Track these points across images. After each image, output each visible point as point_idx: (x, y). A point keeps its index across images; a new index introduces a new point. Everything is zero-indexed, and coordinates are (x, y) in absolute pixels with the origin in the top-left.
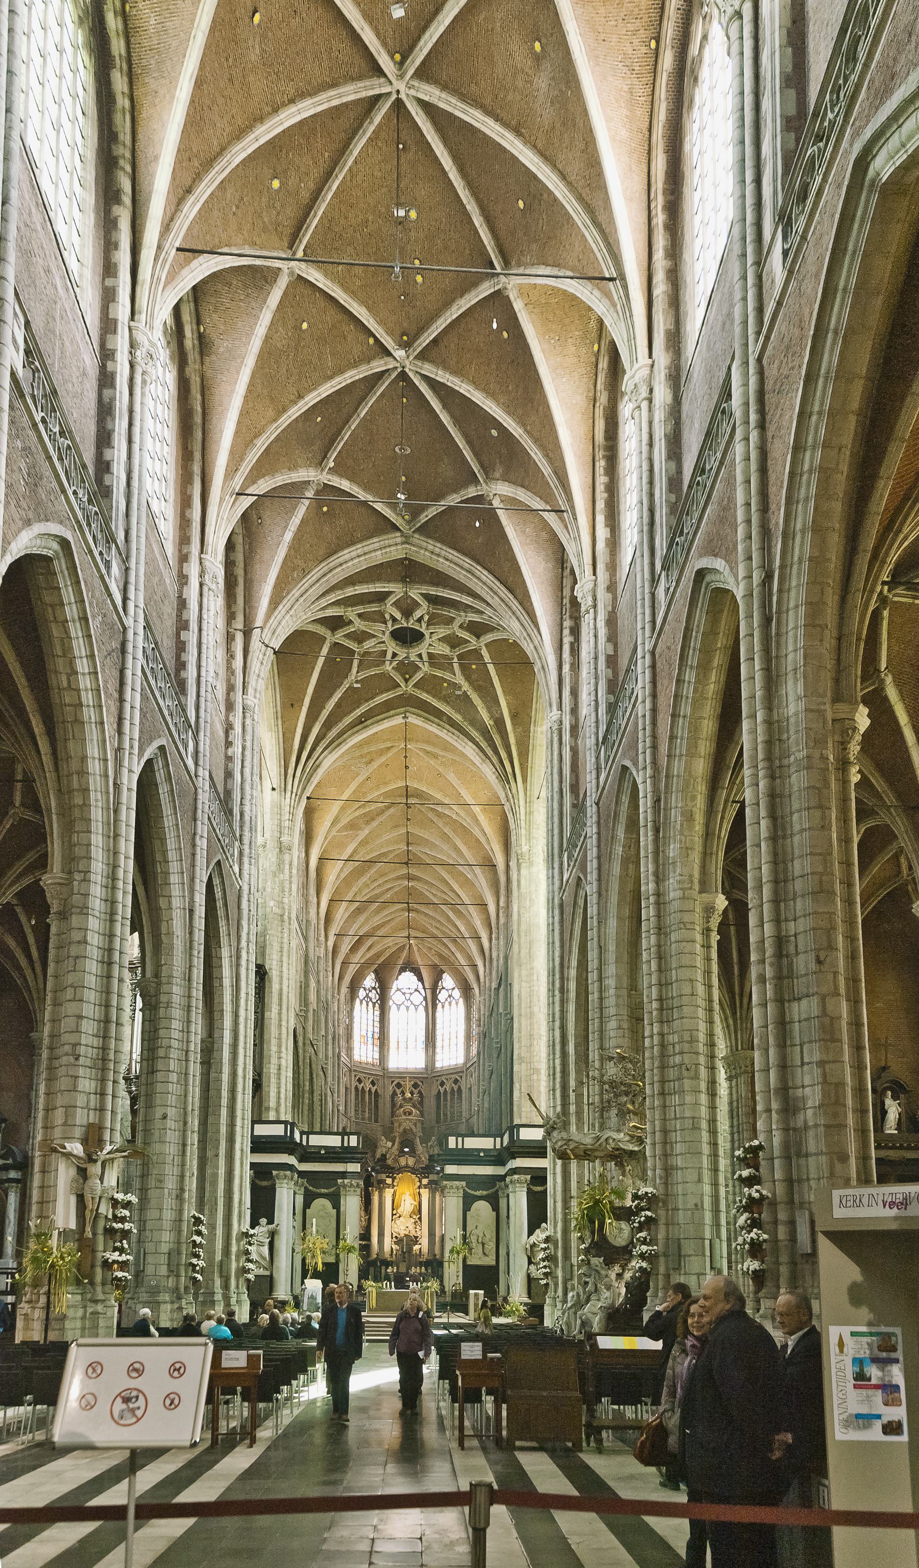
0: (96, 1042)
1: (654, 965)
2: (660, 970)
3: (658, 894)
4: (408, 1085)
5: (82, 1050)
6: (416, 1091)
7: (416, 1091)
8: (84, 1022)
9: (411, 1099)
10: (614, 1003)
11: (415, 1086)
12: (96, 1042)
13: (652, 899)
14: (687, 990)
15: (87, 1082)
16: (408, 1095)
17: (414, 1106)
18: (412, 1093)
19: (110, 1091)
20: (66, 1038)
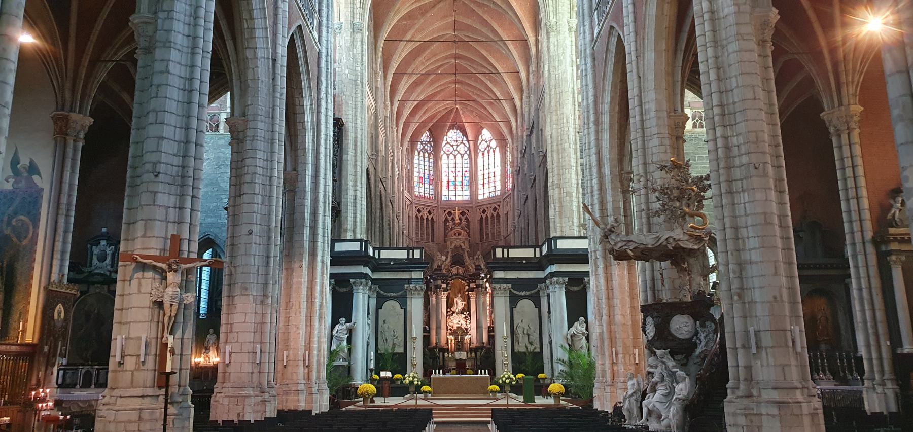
0: (177, 161)
1: (713, 75)
2: (719, 79)
3: (712, 12)
4: (457, 213)
5: (162, 168)
6: (463, 218)
7: (463, 218)
8: (165, 142)
9: (460, 223)
10: (655, 124)
11: (463, 213)
12: (177, 161)
13: (706, 16)
14: (750, 95)
15: (166, 197)
16: (457, 221)
17: (462, 228)
18: (460, 219)
19: (188, 204)
20: (148, 157)
